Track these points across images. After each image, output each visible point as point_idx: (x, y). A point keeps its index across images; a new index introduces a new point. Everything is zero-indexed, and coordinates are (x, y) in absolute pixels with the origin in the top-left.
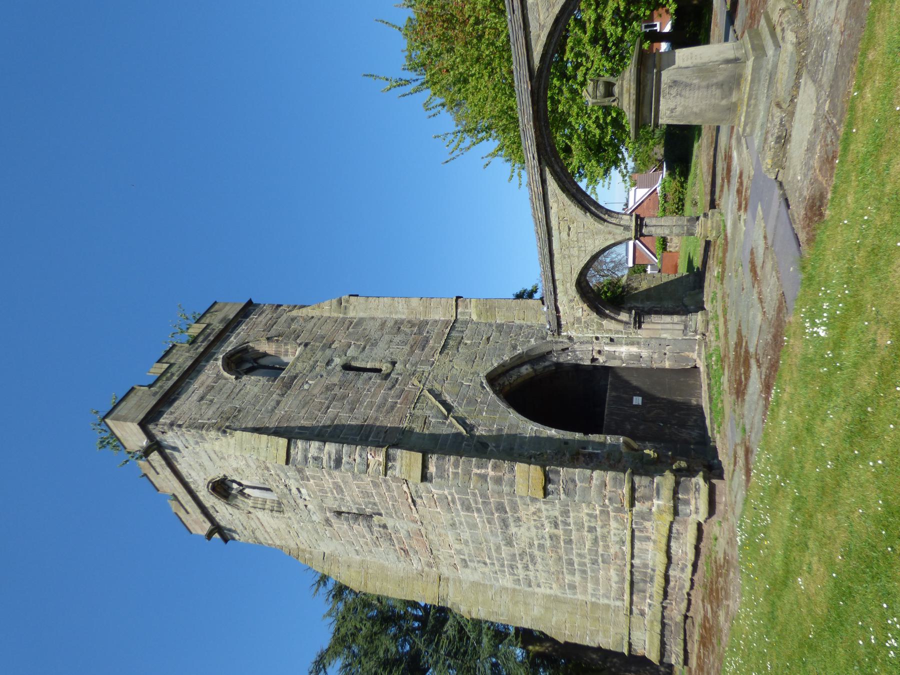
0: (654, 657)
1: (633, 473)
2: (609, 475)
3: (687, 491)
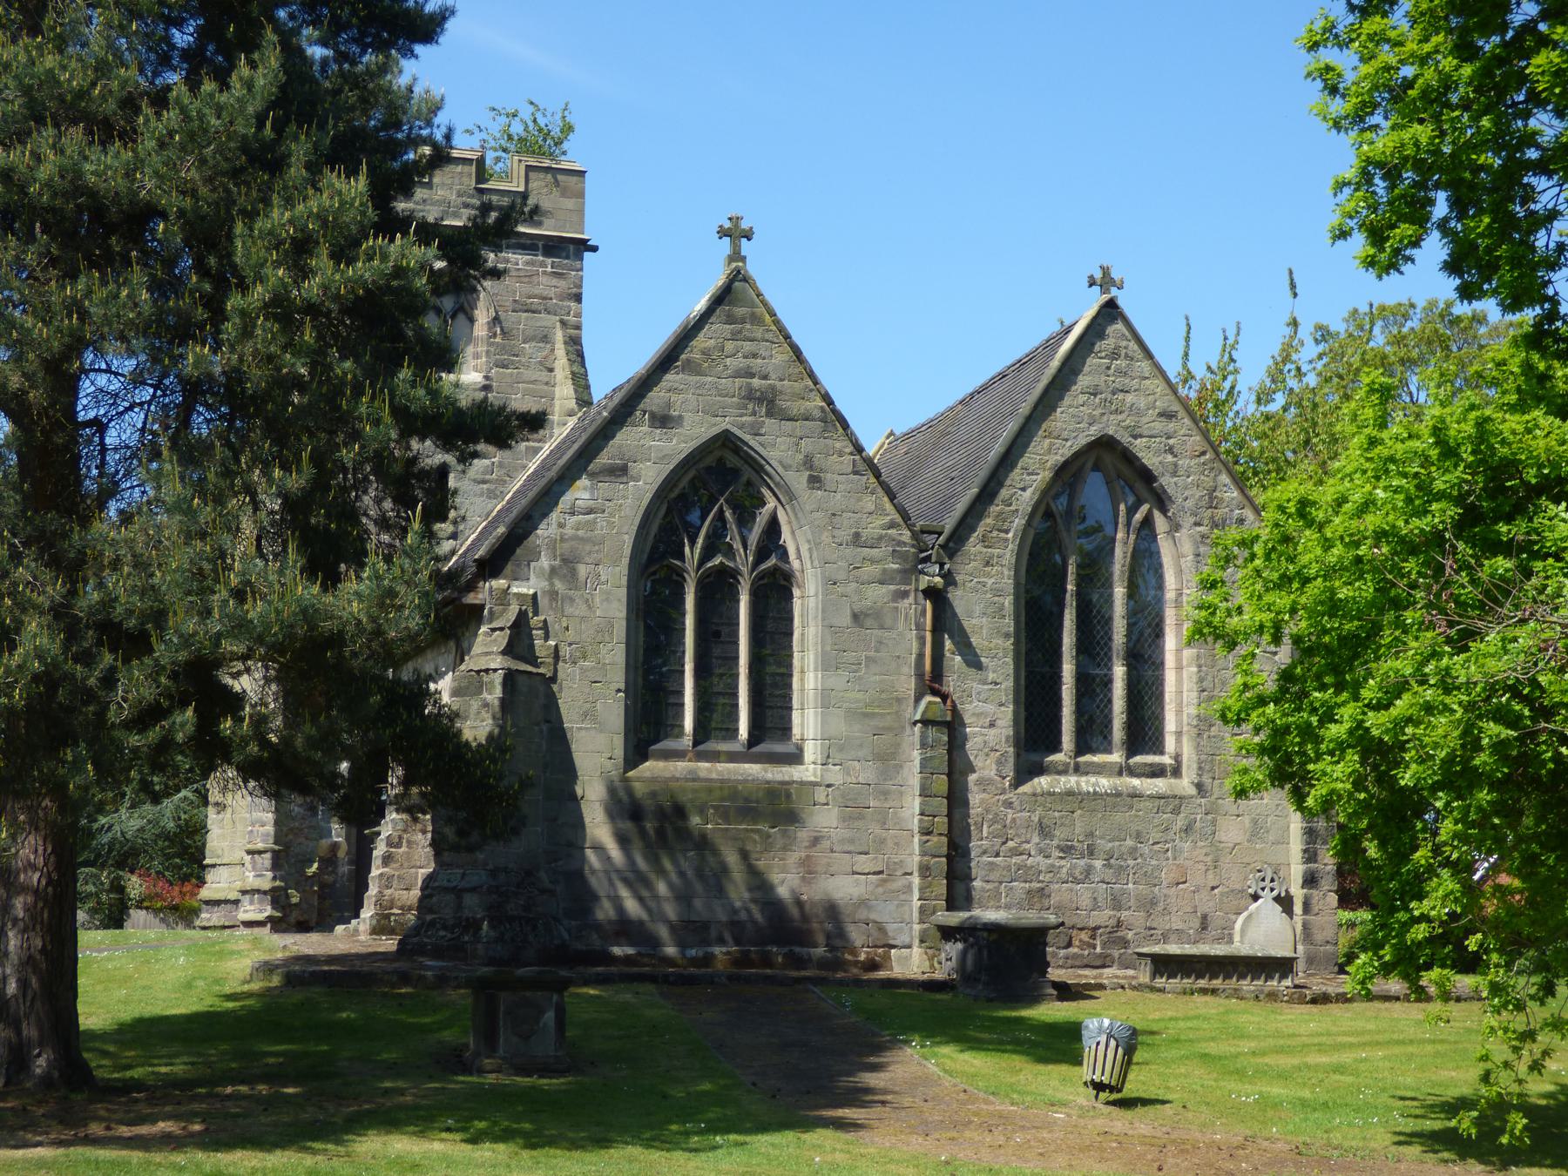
0: (205, 893)
1: (274, 851)
2: (270, 829)
3: (260, 902)
